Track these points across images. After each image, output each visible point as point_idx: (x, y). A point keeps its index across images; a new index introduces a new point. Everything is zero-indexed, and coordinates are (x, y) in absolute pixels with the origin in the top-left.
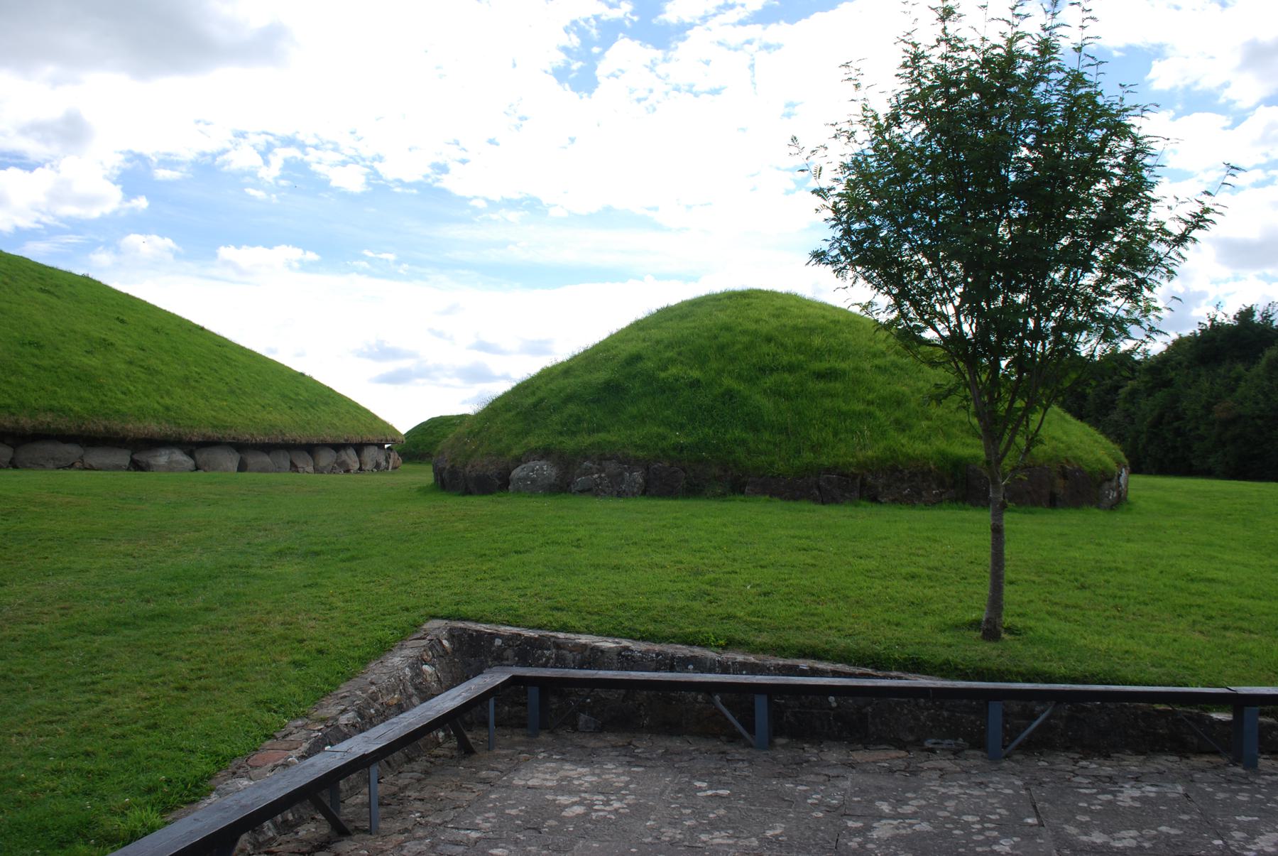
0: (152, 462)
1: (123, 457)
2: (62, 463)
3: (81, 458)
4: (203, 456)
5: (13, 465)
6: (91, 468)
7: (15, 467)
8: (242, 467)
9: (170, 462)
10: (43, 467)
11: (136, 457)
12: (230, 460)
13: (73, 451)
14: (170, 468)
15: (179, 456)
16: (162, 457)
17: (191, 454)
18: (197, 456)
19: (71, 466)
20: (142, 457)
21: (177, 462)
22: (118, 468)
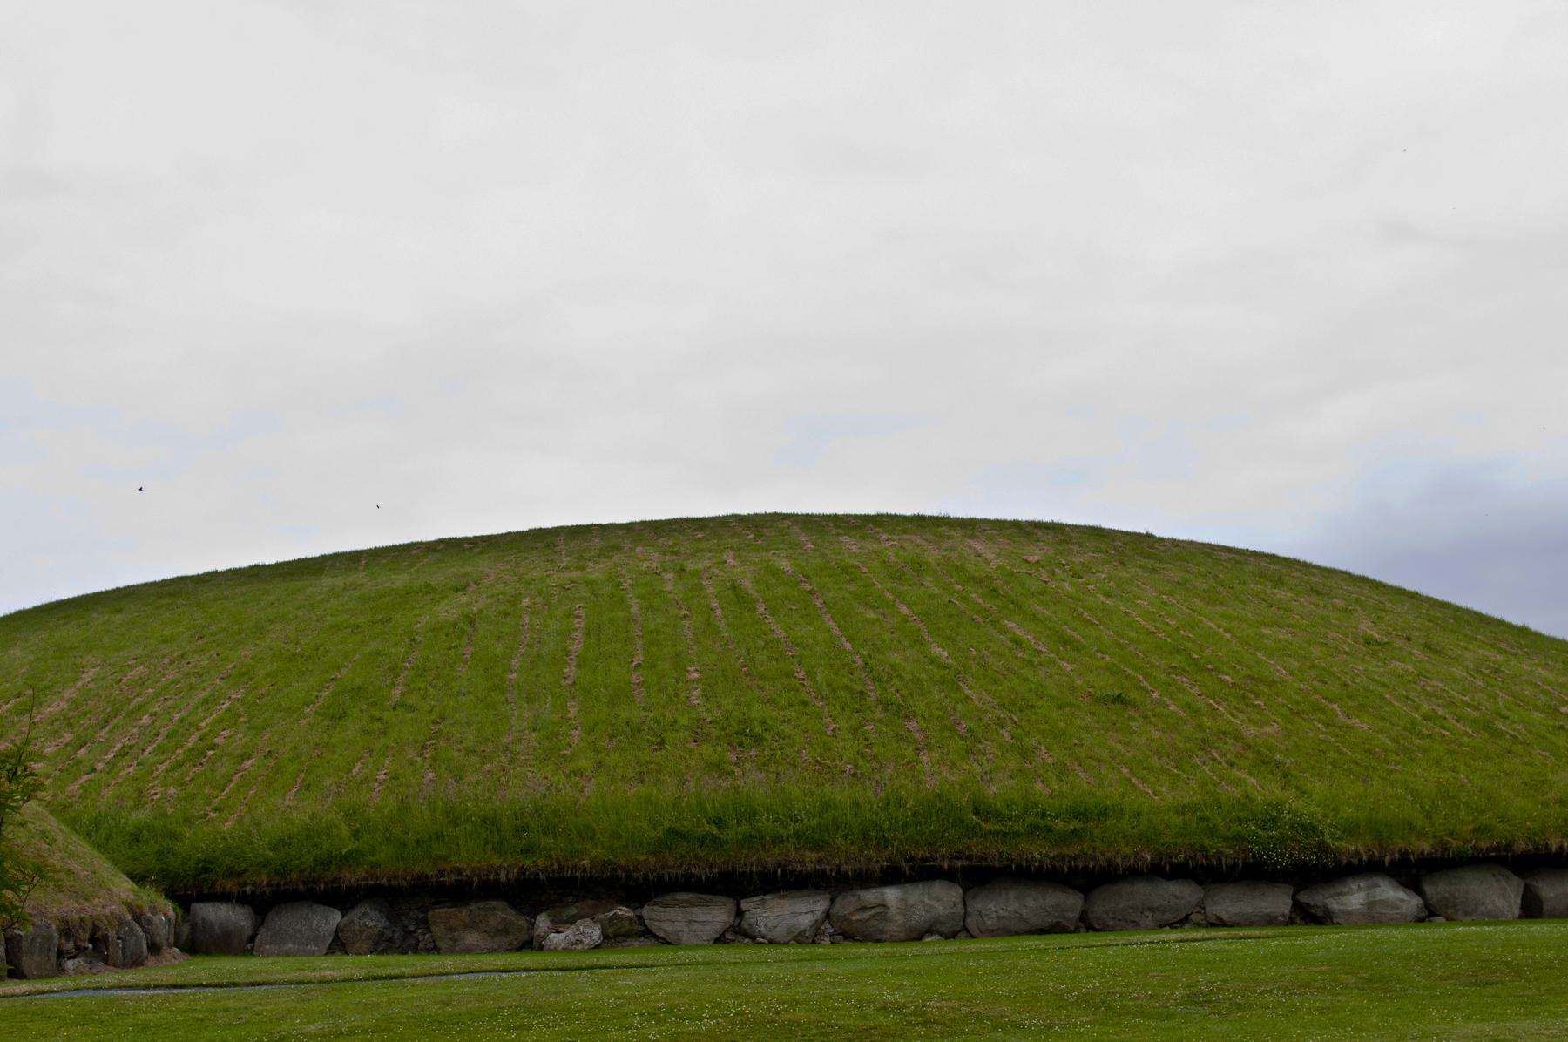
0: (1334, 905)
1: (1278, 901)
2: (1167, 917)
3: (1201, 905)
4: (1437, 889)
5: (1087, 924)
6: (1220, 923)
7: (1090, 928)
8: (1531, 909)
9: (1371, 905)
10: (1136, 926)
11: (1304, 898)
12: (1502, 893)
13: (1182, 893)
14: (1373, 916)
15: (1389, 892)
16: (1354, 897)
17: (1414, 886)
18: (1429, 889)
19: (1182, 922)
20: (1310, 898)
21: (1385, 903)
22: (1270, 921)
